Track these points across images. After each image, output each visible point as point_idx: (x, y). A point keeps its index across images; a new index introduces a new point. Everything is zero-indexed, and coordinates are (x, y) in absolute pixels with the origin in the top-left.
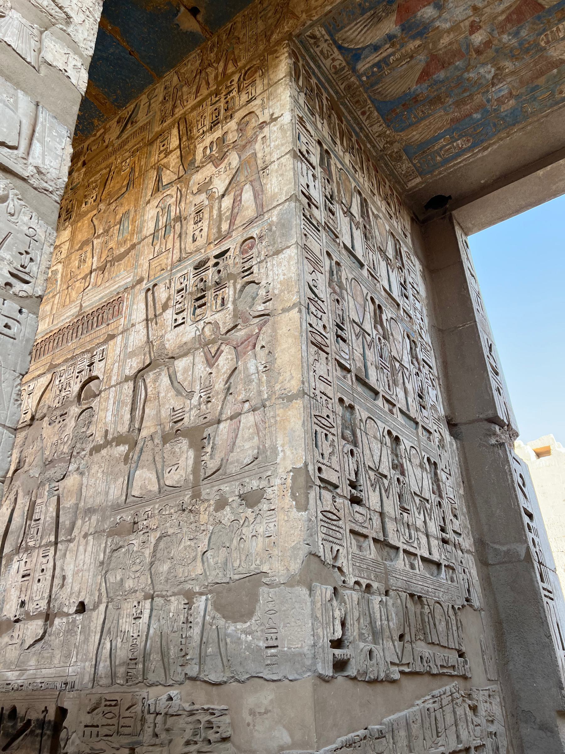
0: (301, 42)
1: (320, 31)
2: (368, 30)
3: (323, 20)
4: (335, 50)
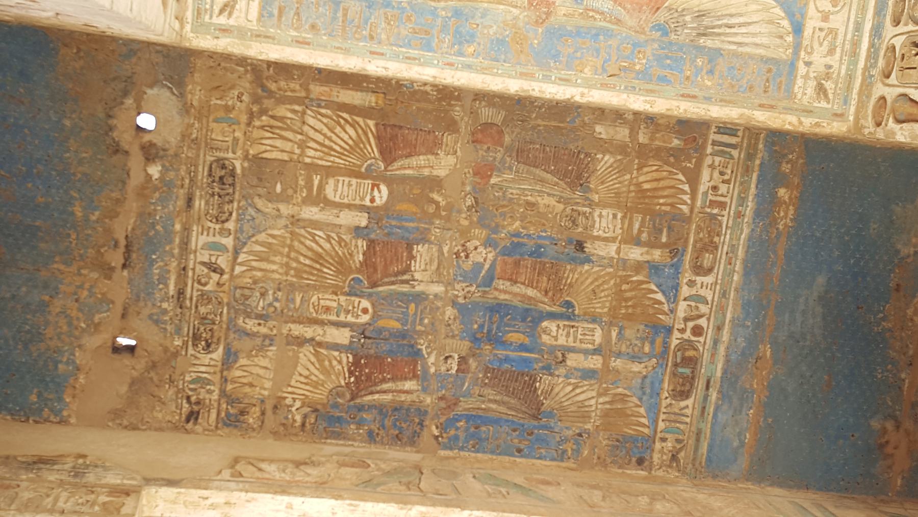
0: (846, 102)
1: (804, 90)
2: (731, 16)
3: (784, 103)
4: (808, 32)
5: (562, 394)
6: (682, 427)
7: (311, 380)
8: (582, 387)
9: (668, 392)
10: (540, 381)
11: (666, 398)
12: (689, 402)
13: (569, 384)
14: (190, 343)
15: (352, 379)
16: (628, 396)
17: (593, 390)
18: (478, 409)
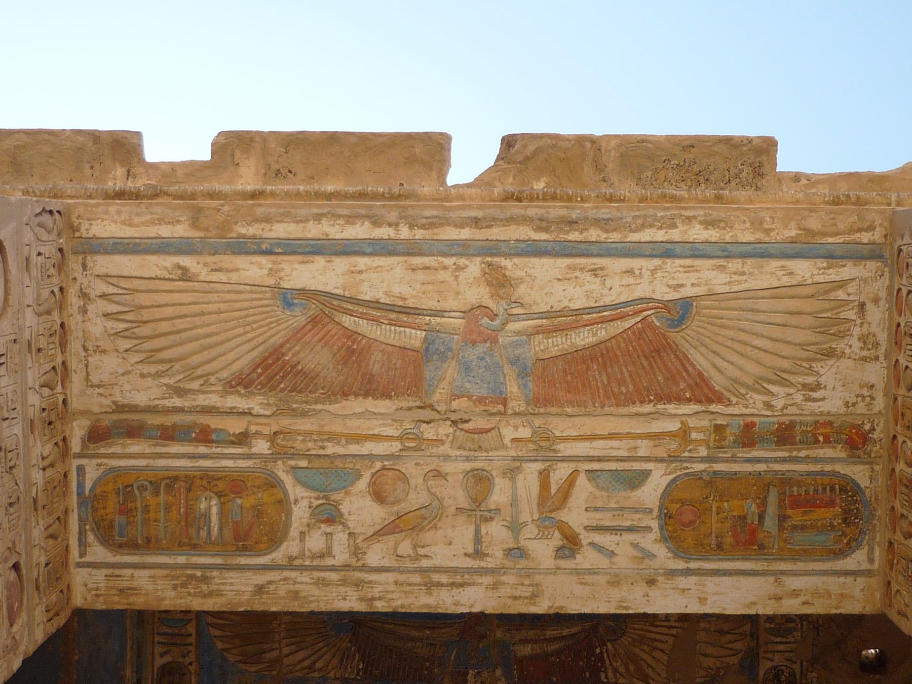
5: (327, 657)
6: (164, 629)
7: (649, 646)
8: (304, 668)
9: (190, 673)
10: (358, 670)
11: (190, 664)
12: (159, 662)
13: (320, 670)
14: (798, 677)
15: (598, 651)
16: (240, 662)
17: (289, 666)
18: (434, 628)
